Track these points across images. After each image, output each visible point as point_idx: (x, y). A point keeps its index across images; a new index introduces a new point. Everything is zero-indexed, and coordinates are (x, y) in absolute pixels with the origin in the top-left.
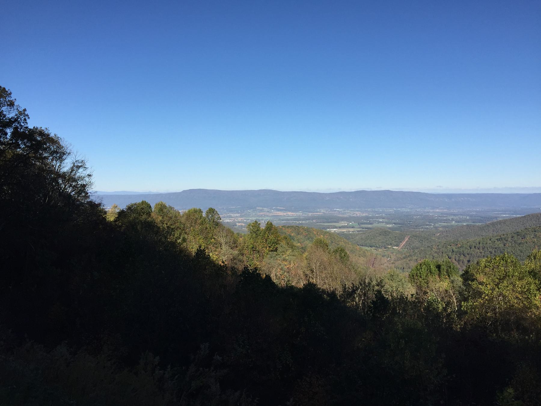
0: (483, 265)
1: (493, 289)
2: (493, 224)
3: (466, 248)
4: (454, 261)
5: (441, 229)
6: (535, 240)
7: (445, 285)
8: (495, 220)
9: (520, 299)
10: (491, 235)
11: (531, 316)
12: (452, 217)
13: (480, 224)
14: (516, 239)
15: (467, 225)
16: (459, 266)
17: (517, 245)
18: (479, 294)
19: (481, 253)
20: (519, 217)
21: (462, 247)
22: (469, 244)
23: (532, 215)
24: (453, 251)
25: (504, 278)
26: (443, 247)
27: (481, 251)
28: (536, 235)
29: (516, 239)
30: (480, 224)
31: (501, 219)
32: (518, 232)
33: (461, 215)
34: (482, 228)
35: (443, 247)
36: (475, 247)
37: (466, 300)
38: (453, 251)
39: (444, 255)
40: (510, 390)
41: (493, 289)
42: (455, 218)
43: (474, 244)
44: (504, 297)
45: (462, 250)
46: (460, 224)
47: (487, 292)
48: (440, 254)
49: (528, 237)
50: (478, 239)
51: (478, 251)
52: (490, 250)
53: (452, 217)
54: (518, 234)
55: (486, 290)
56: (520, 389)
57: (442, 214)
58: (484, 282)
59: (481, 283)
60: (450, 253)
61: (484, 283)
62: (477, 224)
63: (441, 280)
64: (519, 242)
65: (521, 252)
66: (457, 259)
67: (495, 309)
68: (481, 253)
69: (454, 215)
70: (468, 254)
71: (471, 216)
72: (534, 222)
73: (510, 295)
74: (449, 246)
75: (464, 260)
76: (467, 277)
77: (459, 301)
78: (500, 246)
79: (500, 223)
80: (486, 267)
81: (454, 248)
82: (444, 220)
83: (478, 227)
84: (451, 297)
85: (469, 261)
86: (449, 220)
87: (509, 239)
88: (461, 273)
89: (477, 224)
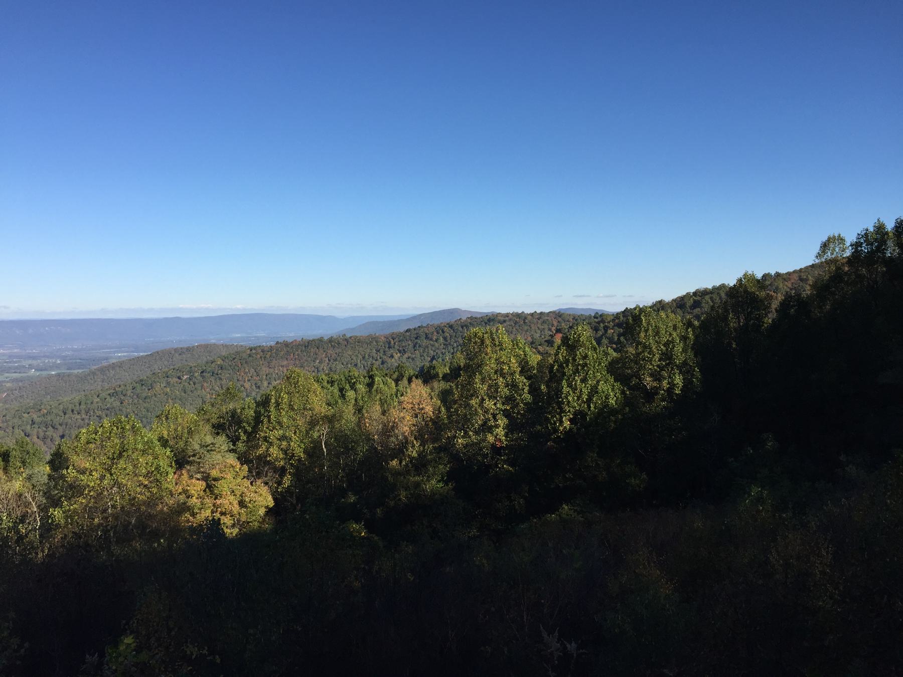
0: (83, 439)
1: (102, 478)
2: (102, 370)
3: (57, 415)
4: (35, 439)
5: (8, 385)
6: (168, 390)
7: (17, 485)
8: (105, 363)
9: (145, 486)
10: (99, 388)
11: (162, 510)
12: (30, 362)
13: (80, 371)
14: (138, 390)
15: (58, 375)
16: (44, 448)
17: (141, 401)
18: (75, 490)
19: (83, 420)
20: (142, 356)
21: (49, 413)
22: (61, 407)
23: (163, 352)
24: (33, 423)
25: (120, 455)
26: (14, 417)
27: (84, 416)
28: (168, 383)
29: (138, 390)
30: (80, 371)
31: (114, 361)
32: (141, 380)
33: (45, 356)
34: (82, 379)
35: (14, 417)
36: (73, 411)
37: (56, 503)
38: (33, 423)
39: (17, 431)
40: (129, 640)
41: (102, 478)
42: (35, 362)
43: (70, 407)
44: (120, 486)
45: (49, 418)
46: (45, 373)
47: (92, 484)
48: (10, 430)
49: (157, 387)
50: (77, 397)
51: (79, 417)
52: (99, 413)
53: (30, 362)
54: (142, 382)
55: (91, 481)
56: (144, 633)
57: (10, 357)
58: (86, 468)
59: (83, 472)
60: (29, 427)
61: (87, 469)
62: (76, 371)
63: (10, 479)
64: (144, 395)
65: (148, 411)
66: (42, 435)
67: (105, 511)
68: (83, 420)
69: (34, 358)
70: (61, 425)
71: (64, 358)
72: (166, 363)
73: (131, 482)
74: (25, 415)
75: (55, 435)
76: (58, 461)
77: (43, 509)
78: (115, 405)
79: (113, 366)
80: (88, 443)
81: (35, 416)
82: (17, 368)
83: (77, 376)
84: (27, 505)
85: (62, 437)
86: (24, 367)
87: (129, 393)
88: (48, 458)
89: (76, 371)
